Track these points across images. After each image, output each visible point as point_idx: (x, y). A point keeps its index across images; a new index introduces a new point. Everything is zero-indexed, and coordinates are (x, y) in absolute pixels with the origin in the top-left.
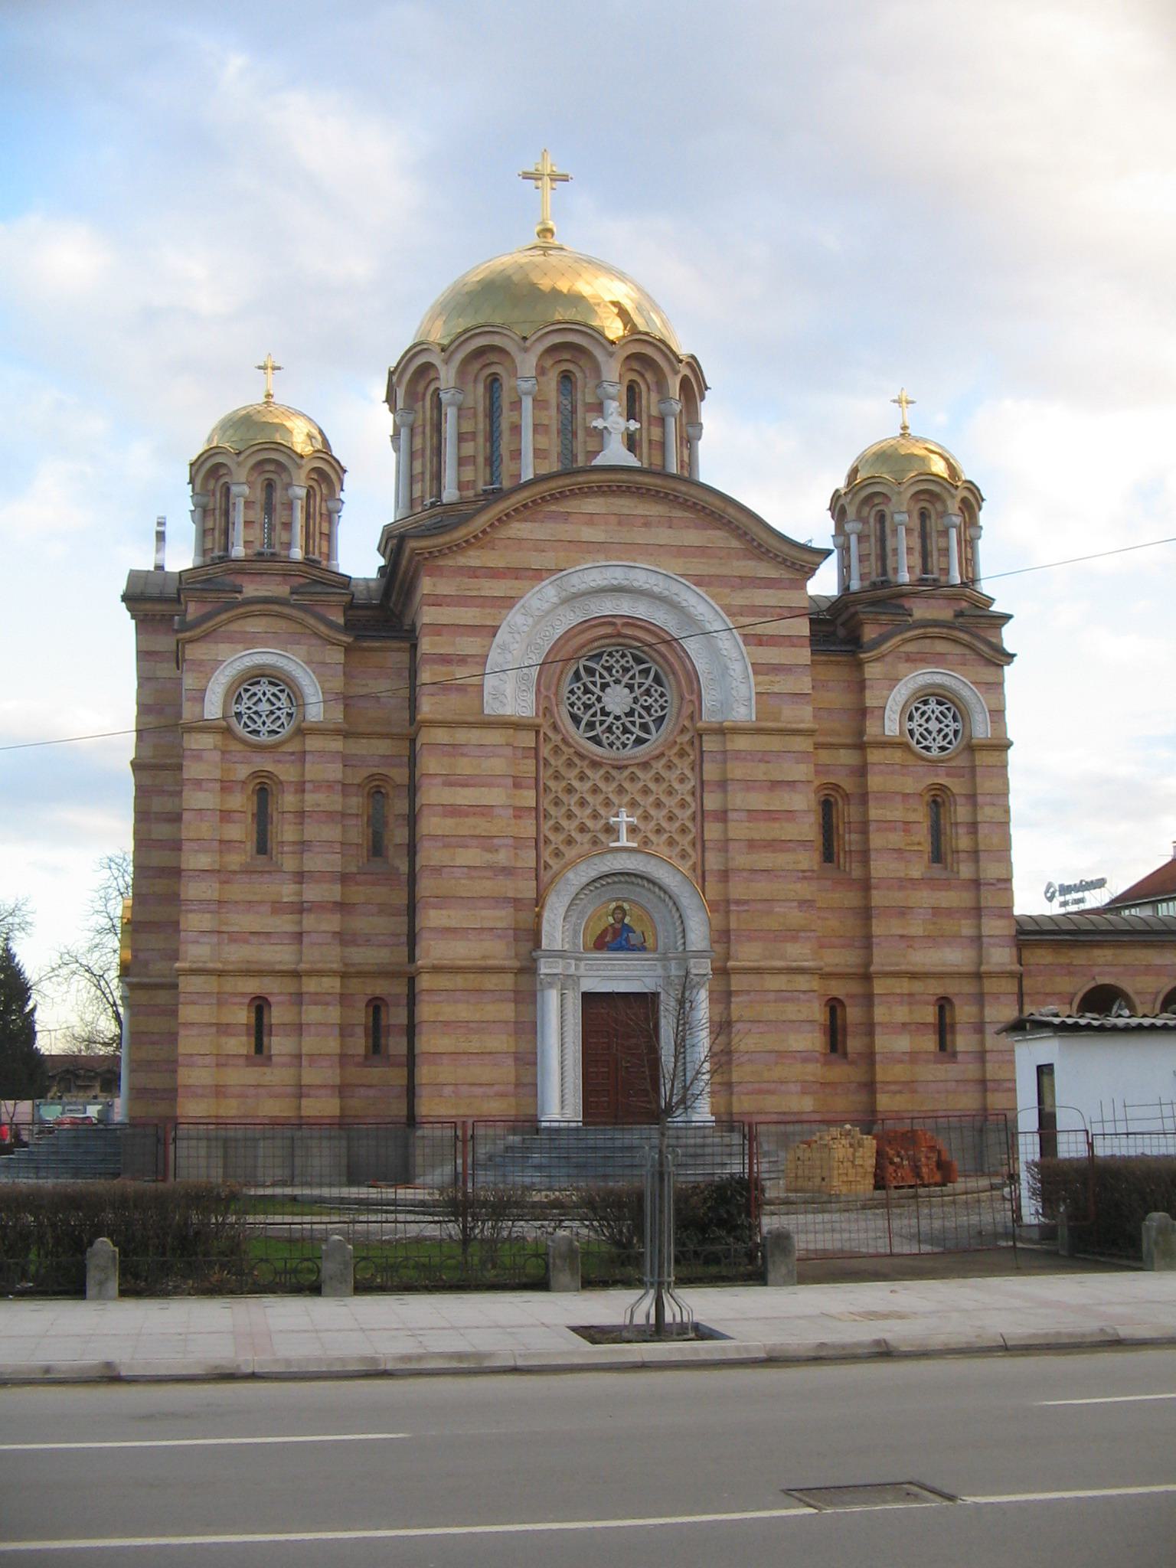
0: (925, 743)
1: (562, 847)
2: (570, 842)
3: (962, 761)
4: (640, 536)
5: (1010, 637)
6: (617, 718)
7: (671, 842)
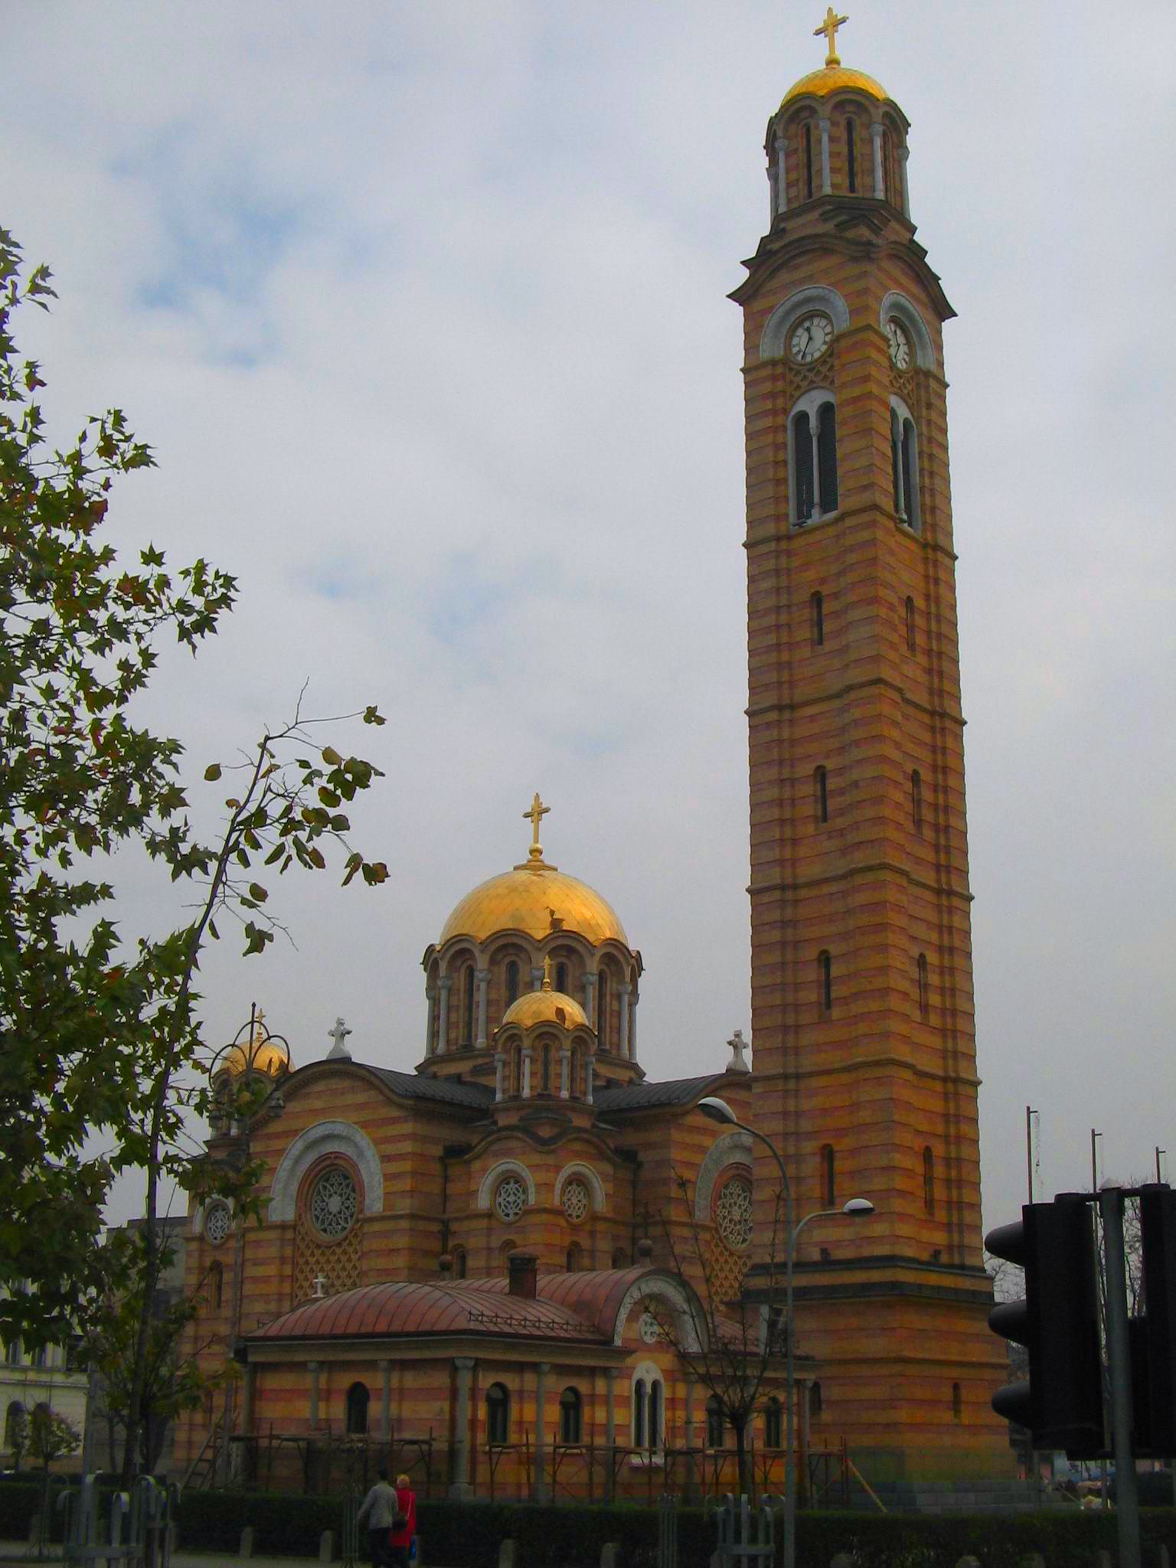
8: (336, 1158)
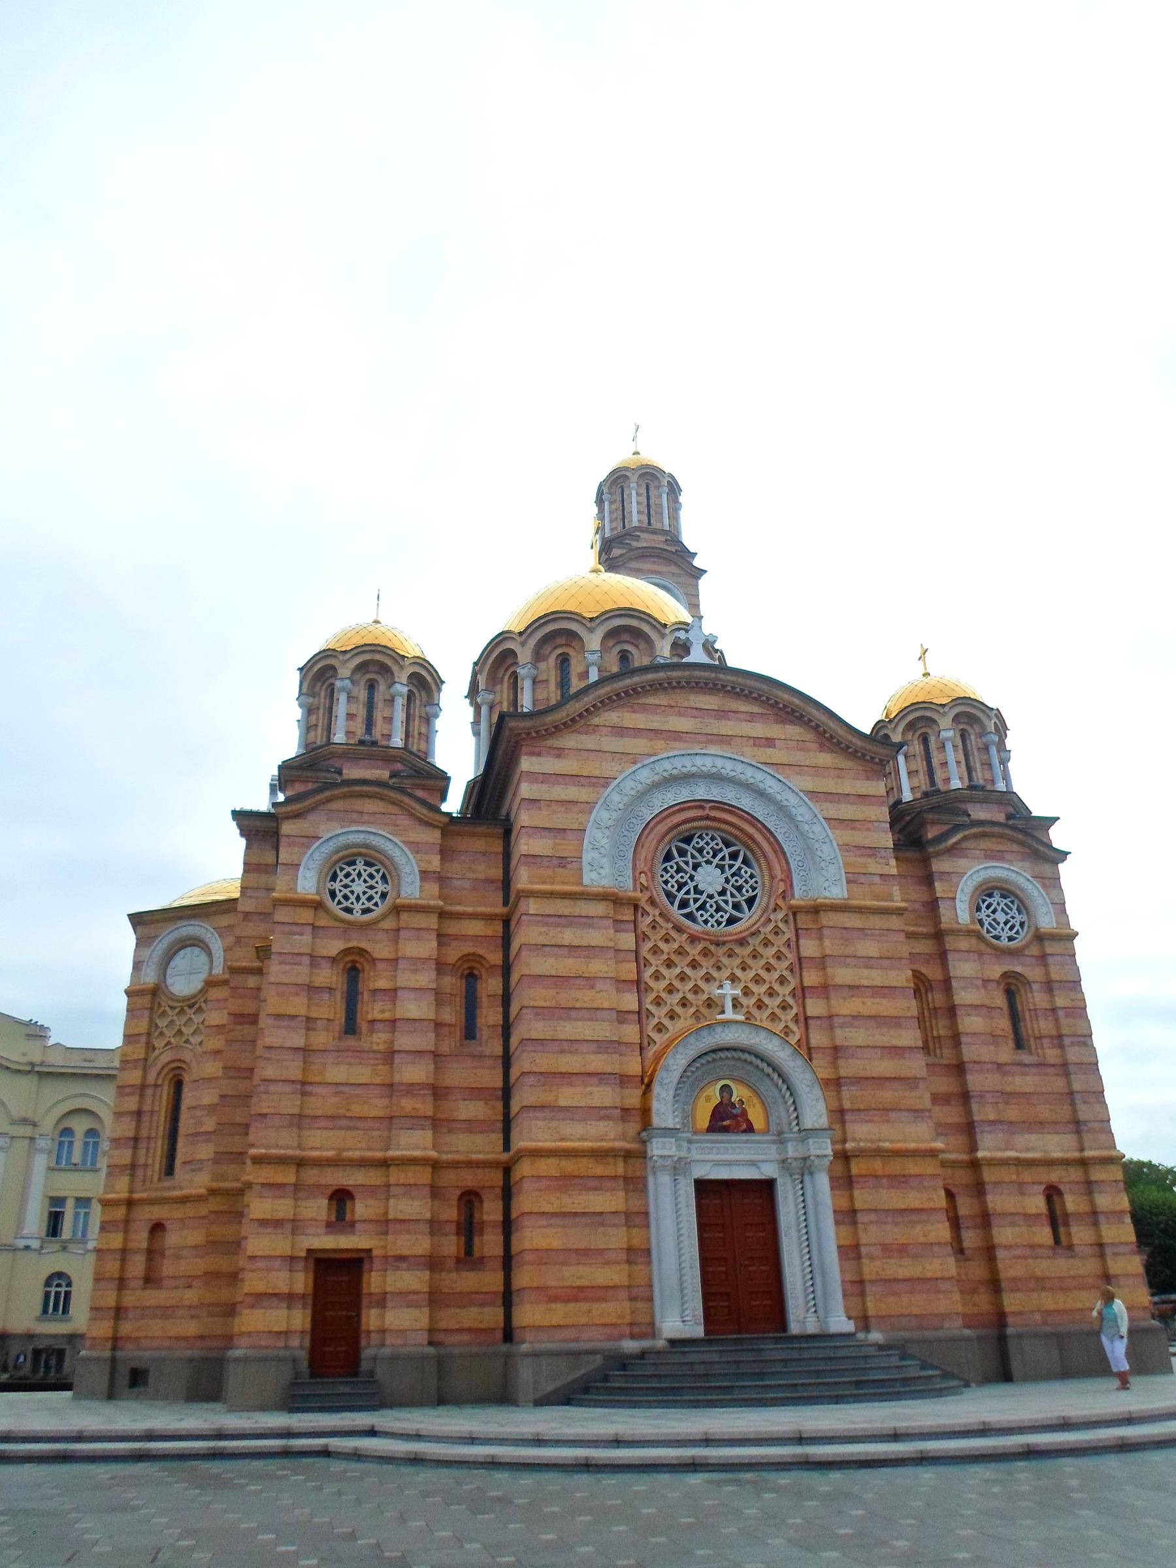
0: (994, 933)
1: (666, 1022)
2: (672, 1016)
3: (1034, 950)
4: (727, 727)
5: (1058, 837)
6: (711, 897)
7: (773, 1017)
8: (711, 808)
